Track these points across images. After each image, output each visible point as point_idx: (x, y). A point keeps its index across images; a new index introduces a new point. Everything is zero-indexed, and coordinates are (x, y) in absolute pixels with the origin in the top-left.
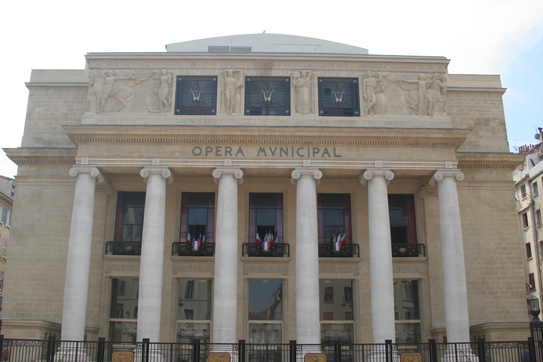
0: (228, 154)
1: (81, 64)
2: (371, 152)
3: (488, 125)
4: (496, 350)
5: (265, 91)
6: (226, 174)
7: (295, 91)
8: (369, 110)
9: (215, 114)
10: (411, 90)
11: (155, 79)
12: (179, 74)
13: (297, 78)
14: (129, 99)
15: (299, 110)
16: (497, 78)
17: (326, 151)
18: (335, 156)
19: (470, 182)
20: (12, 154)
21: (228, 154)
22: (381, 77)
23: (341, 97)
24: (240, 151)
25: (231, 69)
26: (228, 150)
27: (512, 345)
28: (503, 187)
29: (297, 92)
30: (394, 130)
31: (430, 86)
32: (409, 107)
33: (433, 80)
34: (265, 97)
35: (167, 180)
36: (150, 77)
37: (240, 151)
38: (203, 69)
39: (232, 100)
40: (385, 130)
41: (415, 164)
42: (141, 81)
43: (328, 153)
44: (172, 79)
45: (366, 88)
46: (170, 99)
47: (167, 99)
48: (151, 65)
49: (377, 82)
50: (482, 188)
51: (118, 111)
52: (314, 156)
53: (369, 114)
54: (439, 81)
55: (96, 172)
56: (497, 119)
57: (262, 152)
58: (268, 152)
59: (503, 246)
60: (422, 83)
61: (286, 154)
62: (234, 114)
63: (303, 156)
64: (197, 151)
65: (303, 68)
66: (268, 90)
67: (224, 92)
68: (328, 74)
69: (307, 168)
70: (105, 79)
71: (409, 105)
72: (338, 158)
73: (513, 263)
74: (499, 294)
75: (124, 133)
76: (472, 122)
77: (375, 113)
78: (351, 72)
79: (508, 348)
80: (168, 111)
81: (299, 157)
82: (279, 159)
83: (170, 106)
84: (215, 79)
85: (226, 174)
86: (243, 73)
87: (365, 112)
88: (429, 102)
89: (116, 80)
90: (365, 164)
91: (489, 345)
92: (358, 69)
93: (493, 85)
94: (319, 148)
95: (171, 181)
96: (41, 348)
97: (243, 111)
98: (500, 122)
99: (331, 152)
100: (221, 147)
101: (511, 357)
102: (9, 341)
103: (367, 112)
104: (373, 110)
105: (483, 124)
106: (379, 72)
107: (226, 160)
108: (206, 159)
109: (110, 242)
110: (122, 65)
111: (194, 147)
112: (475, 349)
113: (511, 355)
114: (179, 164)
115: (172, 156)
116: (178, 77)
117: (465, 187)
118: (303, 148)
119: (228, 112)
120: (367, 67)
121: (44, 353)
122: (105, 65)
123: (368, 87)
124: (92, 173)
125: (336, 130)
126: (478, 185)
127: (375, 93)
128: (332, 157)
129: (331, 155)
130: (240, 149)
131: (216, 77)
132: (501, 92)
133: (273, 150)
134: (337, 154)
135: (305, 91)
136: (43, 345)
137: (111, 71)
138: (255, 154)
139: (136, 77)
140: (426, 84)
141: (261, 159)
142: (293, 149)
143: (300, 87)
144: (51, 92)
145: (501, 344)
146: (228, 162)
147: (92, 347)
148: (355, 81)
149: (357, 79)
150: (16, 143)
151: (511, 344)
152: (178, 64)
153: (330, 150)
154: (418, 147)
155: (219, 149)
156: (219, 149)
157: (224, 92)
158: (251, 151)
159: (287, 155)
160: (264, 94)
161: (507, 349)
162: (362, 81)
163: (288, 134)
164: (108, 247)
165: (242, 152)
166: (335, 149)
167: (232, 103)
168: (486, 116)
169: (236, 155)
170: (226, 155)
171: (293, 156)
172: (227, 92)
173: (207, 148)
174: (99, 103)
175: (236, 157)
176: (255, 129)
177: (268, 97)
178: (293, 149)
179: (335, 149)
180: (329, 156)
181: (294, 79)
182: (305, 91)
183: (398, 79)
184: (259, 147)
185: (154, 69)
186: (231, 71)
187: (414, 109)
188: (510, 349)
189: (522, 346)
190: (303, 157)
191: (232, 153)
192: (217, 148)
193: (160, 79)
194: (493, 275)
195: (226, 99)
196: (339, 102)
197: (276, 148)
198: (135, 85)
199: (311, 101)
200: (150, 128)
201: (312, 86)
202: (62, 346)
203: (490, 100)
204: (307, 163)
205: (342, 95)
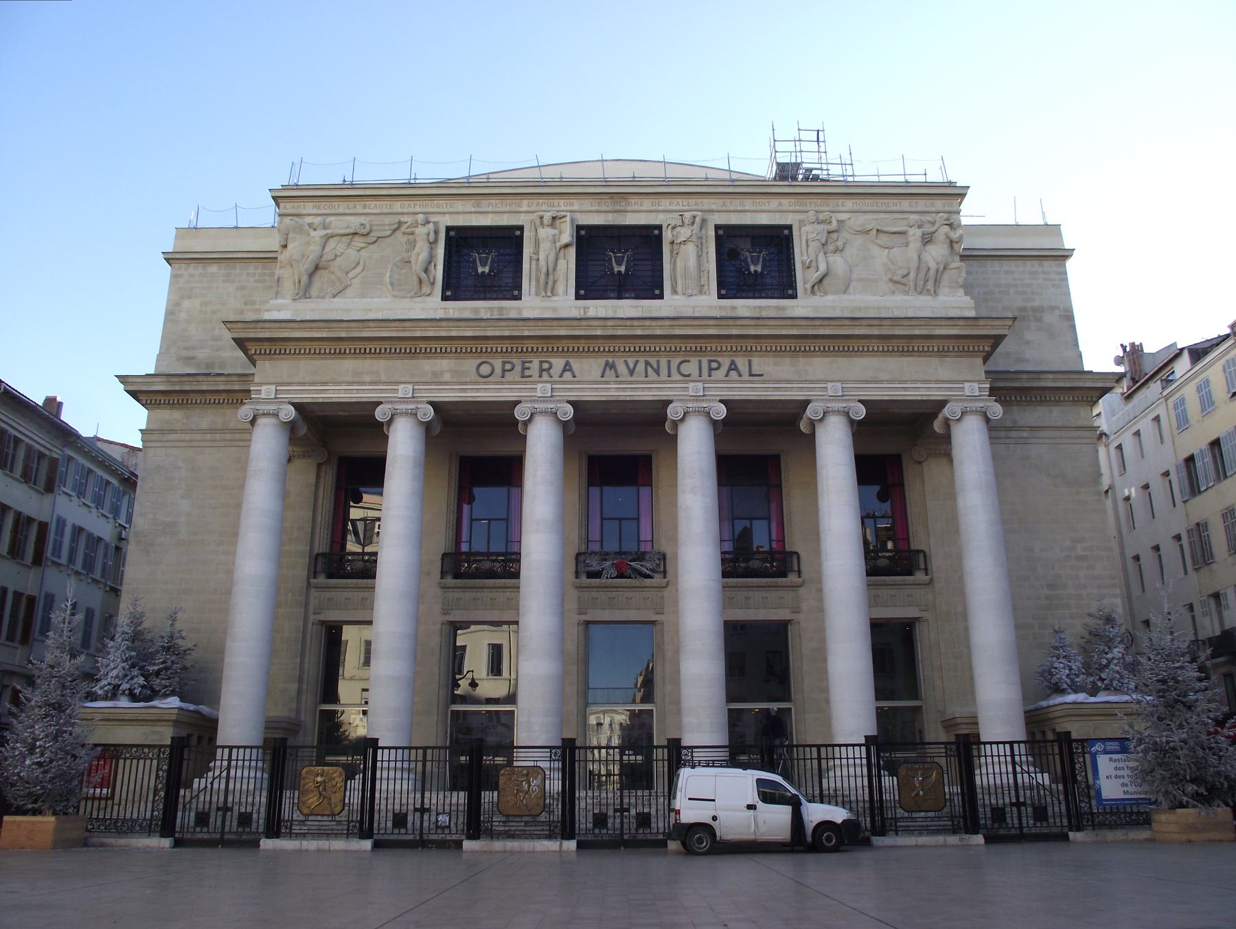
1: (265, 215)
2: (819, 366)
3: (1040, 320)
5: (614, 253)
6: (541, 413)
7: (672, 251)
8: (813, 287)
9: (519, 298)
10: (893, 248)
11: (404, 234)
13: (674, 228)
14: (351, 275)
15: (679, 288)
16: (1054, 230)
17: (733, 367)
18: (751, 375)
20: (138, 390)
23: (760, 263)
24: (567, 368)
25: (549, 211)
26: (546, 366)
30: (864, 322)
31: (927, 239)
32: (891, 280)
33: (937, 226)
34: (614, 264)
36: (395, 231)
37: (567, 368)
39: (550, 271)
40: (847, 322)
42: (378, 238)
43: (736, 369)
44: (436, 232)
45: (808, 246)
46: (433, 271)
47: (426, 271)
48: (398, 206)
49: (829, 232)
51: (334, 296)
52: (710, 376)
53: (813, 292)
54: (947, 229)
56: (1057, 308)
58: (622, 368)
60: (915, 234)
61: (657, 372)
63: (689, 375)
64: (485, 369)
65: (686, 208)
66: (619, 251)
67: (535, 257)
68: (734, 220)
69: (696, 398)
70: (309, 235)
71: (889, 276)
77: (826, 293)
80: (429, 295)
81: (681, 378)
82: (643, 382)
83: (433, 284)
84: (518, 233)
85: (541, 413)
86: (572, 220)
87: (806, 289)
88: (929, 269)
89: (329, 237)
90: (810, 389)
92: (792, 208)
93: (1047, 243)
95: (437, 429)
96: (155, 762)
97: (572, 291)
98: (1062, 313)
99: (743, 367)
100: (531, 362)
103: (809, 290)
106: (831, 214)
107: (539, 386)
108: (502, 383)
110: (342, 207)
111: (479, 361)
116: (448, 229)
118: (688, 361)
119: (543, 294)
120: (808, 205)
121: (161, 773)
122: (309, 207)
123: (811, 244)
125: (752, 322)
127: (825, 253)
128: (746, 377)
129: (742, 372)
130: (567, 364)
131: (521, 228)
132: (1063, 256)
133: (631, 366)
134: (754, 373)
136: (159, 756)
137: (319, 219)
138: (596, 374)
139: (367, 229)
140: (923, 234)
141: (607, 383)
142: (669, 362)
143: (680, 243)
144: (213, 269)
146: (543, 389)
148: (786, 232)
149: (789, 227)
150: (145, 363)
152: (448, 205)
153: (741, 362)
155: (527, 365)
156: (527, 365)
157: (535, 257)
159: (658, 374)
160: (613, 260)
162: (800, 229)
165: (571, 370)
166: (750, 362)
167: (551, 277)
168: (1037, 303)
169: (561, 377)
170: (540, 376)
172: (542, 256)
173: (504, 363)
174: (297, 280)
175: (560, 379)
176: (595, 323)
177: (619, 264)
178: (669, 362)
179: (750, 362)
181: (670, 227)
182: (690, 251)
184: (602, 361)
185: (403, 214)
186: (547, 217)
187: (898, 283)
190: (688, 379)
192: (524, 363)
195: (538, 270)
198: (366, 245)
200: (393, 324)
201: (704, 241)
202: (219, 756)
203: (1043, 273)
204: (695, 388)
205: (761, 260)
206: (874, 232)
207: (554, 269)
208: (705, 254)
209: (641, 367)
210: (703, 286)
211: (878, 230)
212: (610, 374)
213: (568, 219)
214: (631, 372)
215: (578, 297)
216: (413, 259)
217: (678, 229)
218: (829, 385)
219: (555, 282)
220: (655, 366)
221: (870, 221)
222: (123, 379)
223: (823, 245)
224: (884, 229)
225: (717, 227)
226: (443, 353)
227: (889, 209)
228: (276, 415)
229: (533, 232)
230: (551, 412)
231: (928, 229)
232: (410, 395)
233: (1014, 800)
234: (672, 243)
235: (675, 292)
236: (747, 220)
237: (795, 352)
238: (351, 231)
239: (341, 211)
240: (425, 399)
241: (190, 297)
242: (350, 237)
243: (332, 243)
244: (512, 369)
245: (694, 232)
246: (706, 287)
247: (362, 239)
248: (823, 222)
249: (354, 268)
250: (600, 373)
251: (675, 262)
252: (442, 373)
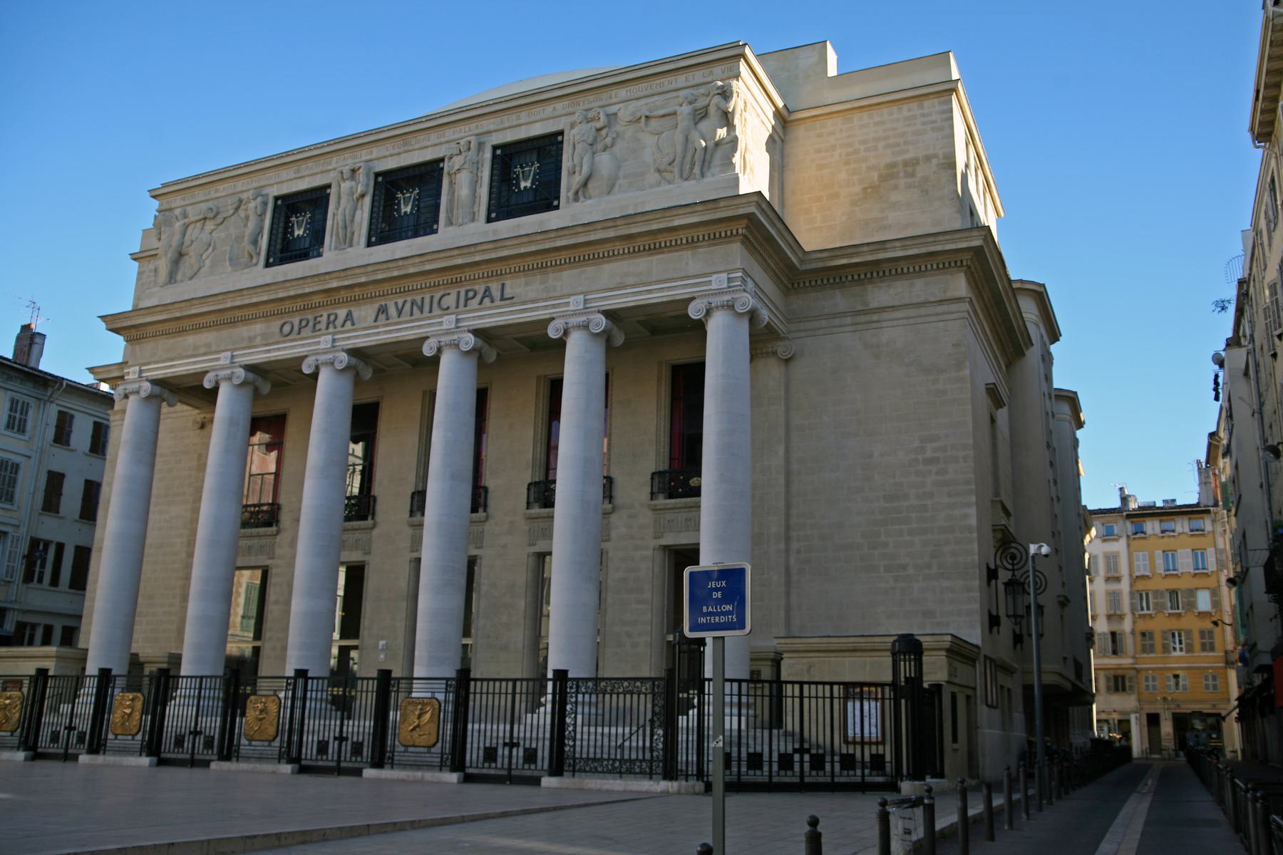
4: (618, 697)
8: (576, 193)
12: (276, 194)
18: (502, 299)
19: (858, 313)
21: (331, 325)
22: (602, 116)
24: (349, 316)
27: (627, 687)
28: (937, 314)
30: (599, 226)
37: (349, 316)
38: (311, 175)
39: (348, 223)
40: (580, 229)
41: (650, 291)
42: (225, 218)
44: (265, 204)
50: (884, 324)
51: (191, 278)
53: (576, 199)
54: (717, 99)
56: (935, 156)
59: (929, 454)
68: (510, 137)
72: (507, 302)
73: (950, 495)
74: (911, 571)
76: (875, 175)
78: (551, 121)
79: (618, 694)
87: (568, 198)
91: (578, 687)
94: (476, 287)
98: (941, 161)
99: (496, 293)
101: (814, 717)
102: (580, 684)
105: (902, 174)
112: (731, 695)
113: (820, 712)
114: (259, 356)
117: (845, 326)
118: (449, 294)
125: (491, 246)
126: (875, 317)
129: (495, 298)
134: (506, 296)
135: (464, 179)
139: (215, 211)
145: (603, 684)
147: (820, 694)
151: (626, 684)
154: (663, 253)
161: (614, 696)
166: (503, 285)
167: (349, 229)
168: (908, 156)
170: (327, 328)
177: (406, 205)
182: (464, 179)
183: (638, 115)
186: (346, 170)
188: (621, 696)
189: (649, 691)
190: (446, 312)
191: (336, 322)
192: (316, 318)
194: (897, 527)
196: (525, 187)
197: (406, 301)
200: (210, 299)
201: (480, 166)
203: (923, 115)
206: (643, 119)
207: (352, 221)
209: (408, 306)
217: (454, 158)
220: (419, 303)
221: (641, 107)
222: (87, 369)
223: (591, 145)
224: (652, 114)
226: (255, 319)
230: (584, 326)
231: (701, 103)
232: (581, 307)
233: (507, 741)
236: (522, 134)
237: (543, 268)
238: (201, 217)
240: (596, 309)
242: (202, 222)
245: (468, 158)
248: (592, 120)
249: (207, 249)
252: (255, 337)
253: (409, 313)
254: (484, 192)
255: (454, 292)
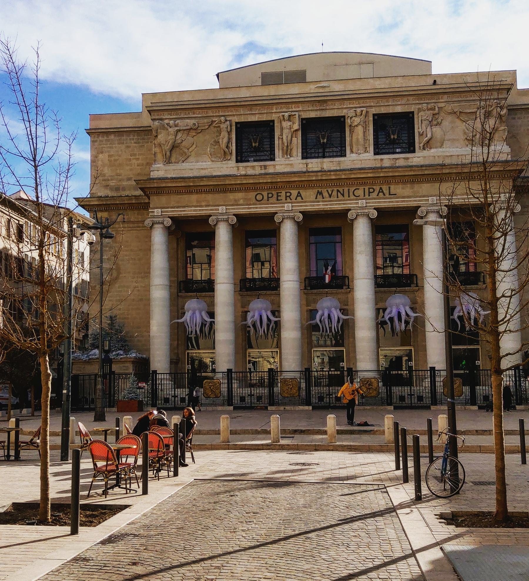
0: (288, 198)
2: (425, 188)
7: (350, 130)
8: (424, 145)
11: (215, 127)
13: (351, 118)
14: (191, 150)
18: (390, 194)
21: (288, 198)
22: (437, 109)
26: (288, 194)
29: (351, 132)
31: (488, 115)
35: (233, 226)
36: (209, 126)
39: (289, 144)
43: (383, 192)
44: (231, 126)
45: (422, 122)
47: (227, 147)
51: (183, 162)
52: (369, 196)
53: (424, 149)
55: (168, 222)
57: (320, 195)
58: (326, 194)
61: (343, 195)
62: (292, 159)
63: (359, 196)
64: (259, 197)
65: (358, 105)
68: (383, 110)
69: (362, 208)
71: (466, 136)
75: (192, 184)
77: (431, 148)
83: (231, 154)
86: (299, 116)
87: (420, 147)
90: (420, 201)
92: (414, 102)
94: (374, 187)
97: (300, 154)
99: (386, 191)
100: (281, 193)
104: (427, 145)
107: (286, 205)
109: (183, 281)
111: (256, 193)
115: (236, 203)
118: (358, 189)
123: (423, 122)
124: (165, 223)
128: (387, 196)
130: (299, 193)
131: (273, 121)
135: (360, 130)
138: (313, 198)
141: (319, 202)
144: (112, 137)
146: (287, 206)
152: (236, 111)
153: (385, 188)
155: (279, 194)
156: (279, 194)
158: (309, 194)
159: (343, 196)
163: (343, 177)
164: (182, 285)
165: (301, 196)
166: (389, 188)
167: (289, 147)
169: (296, 199)
170: (286, 199)
171: (349, 197)
173: (268, 194)
174: (164, 154)
175: (296, 201)
176: (312, 174)
177: (324, 139)
179: (389, 188)
180: (384, 195)
181: (349, 118)
182: (360, 130)
184: (317, 190)
186: (286, 114)
192: (277, 193)
193: (219, 127)
195: (283, 143)
199: (365, 139)
201: (367, 124)
204: (362, 203)
208: (367, 130)
209: (335, 193)
210: (367, 148)
211: (460, 112)
212: (320, 197)
213: (297, 116)
214: (330, 196)
215: (303, 158)
216: (220, 141)
217: (354, 118)
218: (430, 198)
219: (291, 150)
225: (374, 115)
226: (240, 190)
227: (468, 99)
228: (163, 223)
229: (279, 124)
234: (351, 126)
235: (352, 152)
236: (391, 110)
237: (413, 182)
238: (188, 128)
239: (182, 116)
241: (102, 153)
243: (180, 135)
244: (271, 197)
245: (362, 120)
246: (368, 149)
247: (194, 131)
250: (315, 197)
251: (352, 137)
252: (239, 200)
253: (336, 196)
254: (371, 138)
255: (362, 188)
